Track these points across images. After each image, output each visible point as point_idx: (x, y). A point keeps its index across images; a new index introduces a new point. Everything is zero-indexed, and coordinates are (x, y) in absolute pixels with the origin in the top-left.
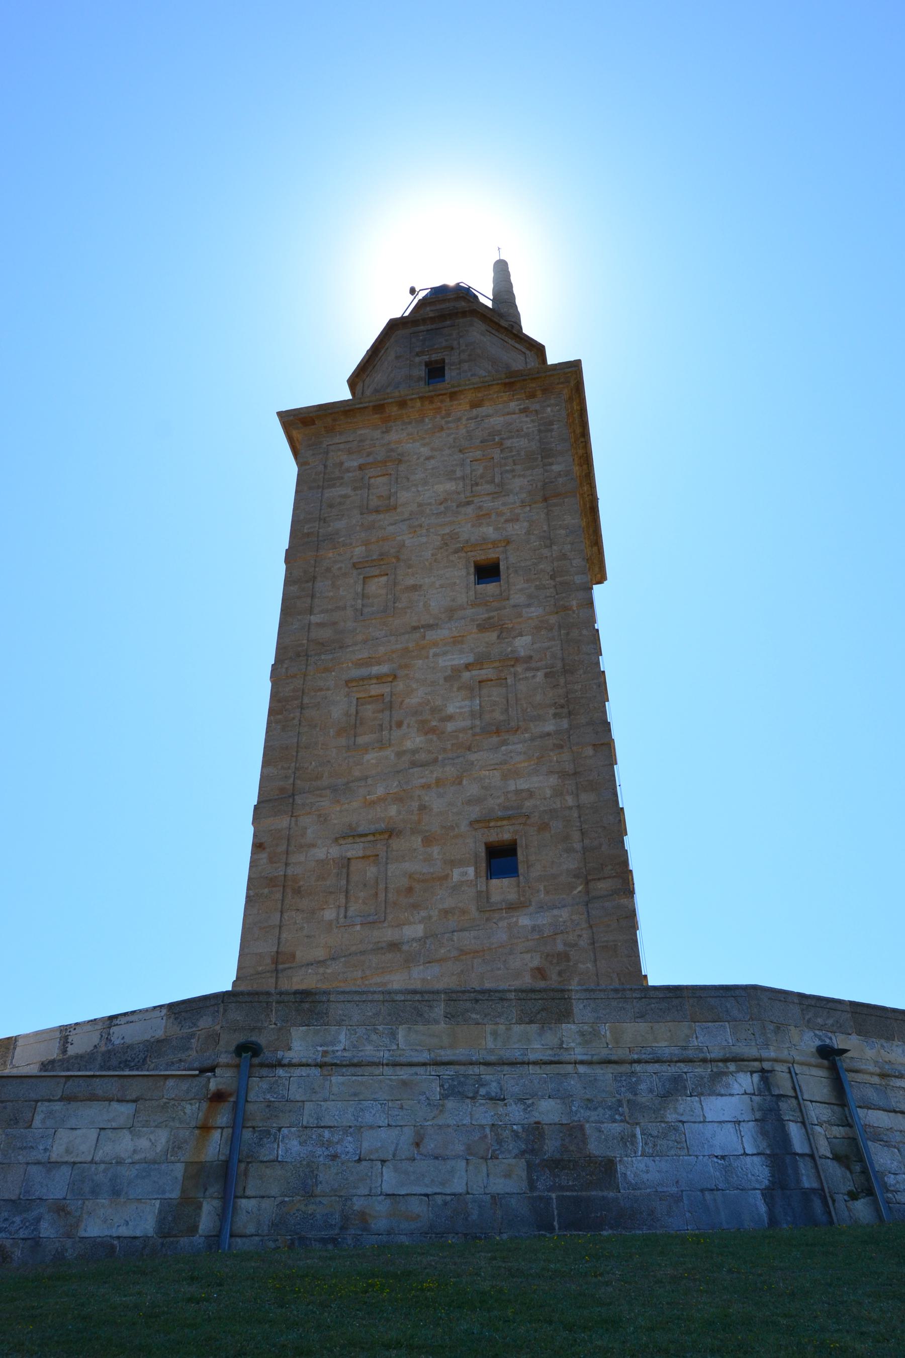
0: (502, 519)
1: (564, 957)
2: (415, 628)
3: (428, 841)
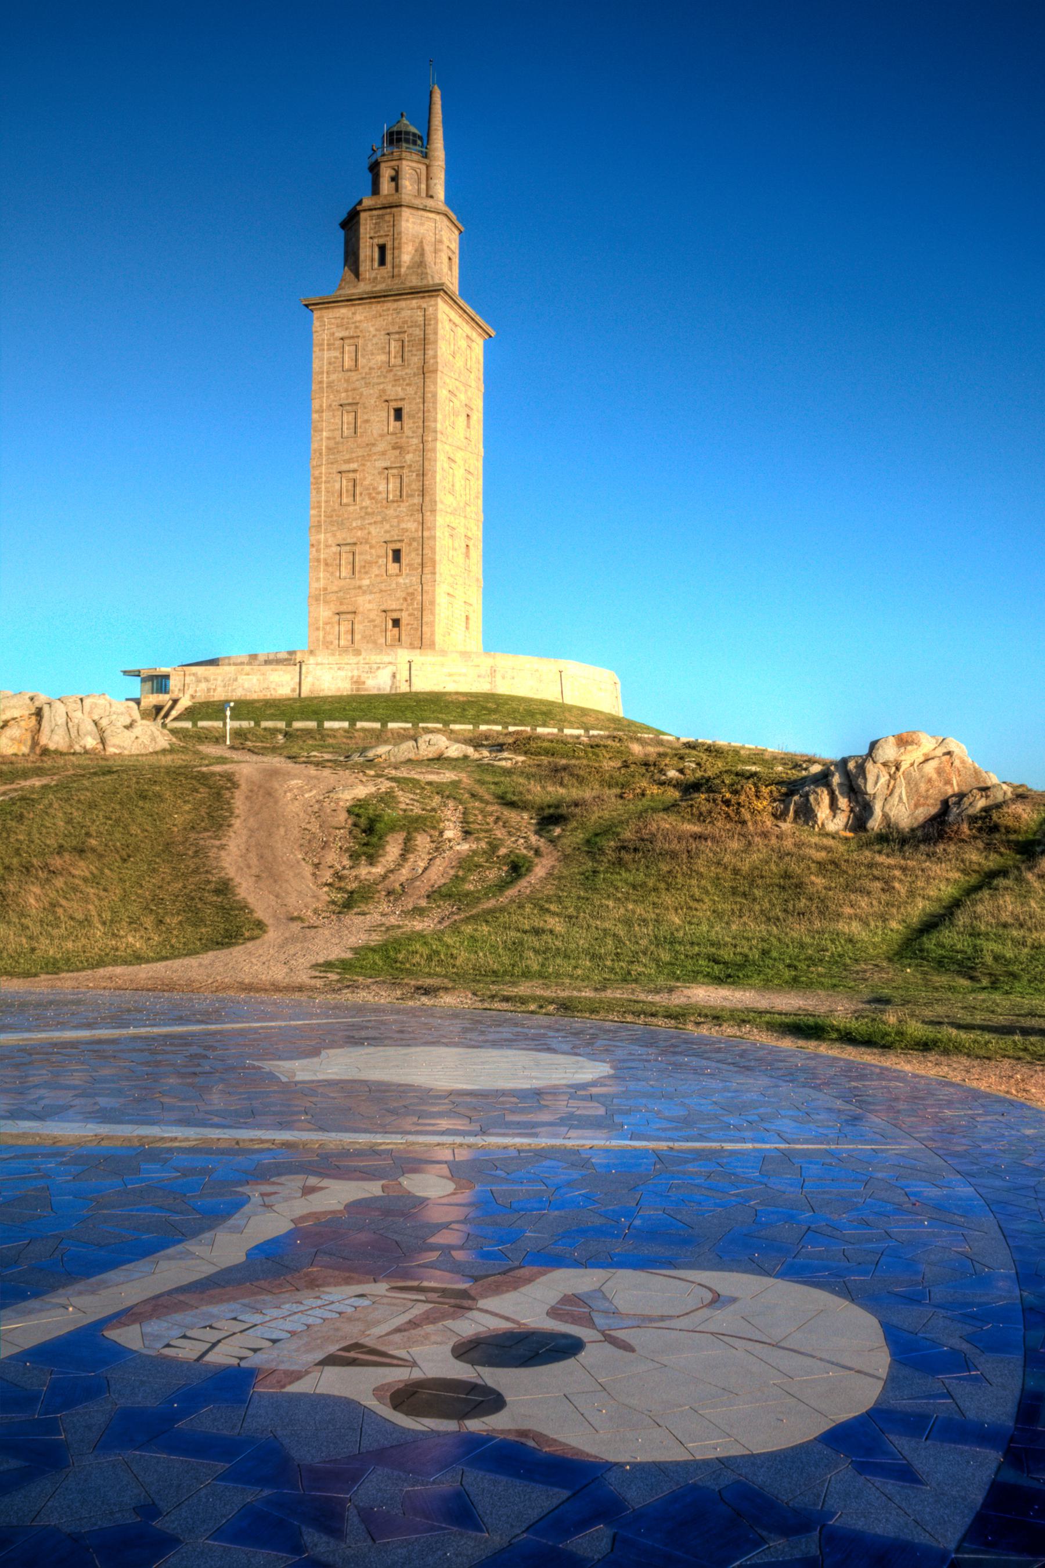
1: (412, 594)
3: (371, 547)
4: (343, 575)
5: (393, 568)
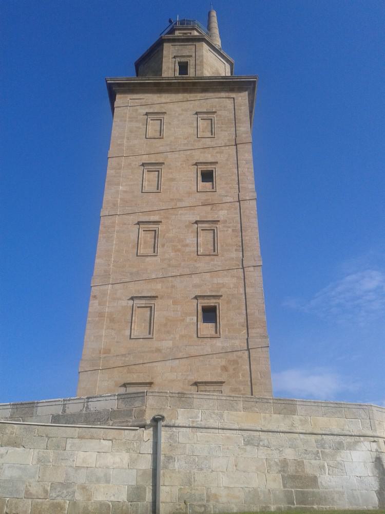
0: (215, 151)
1: (236, 362)
2: (172, 200)
4: (135, 334)
5: (207, 329)
